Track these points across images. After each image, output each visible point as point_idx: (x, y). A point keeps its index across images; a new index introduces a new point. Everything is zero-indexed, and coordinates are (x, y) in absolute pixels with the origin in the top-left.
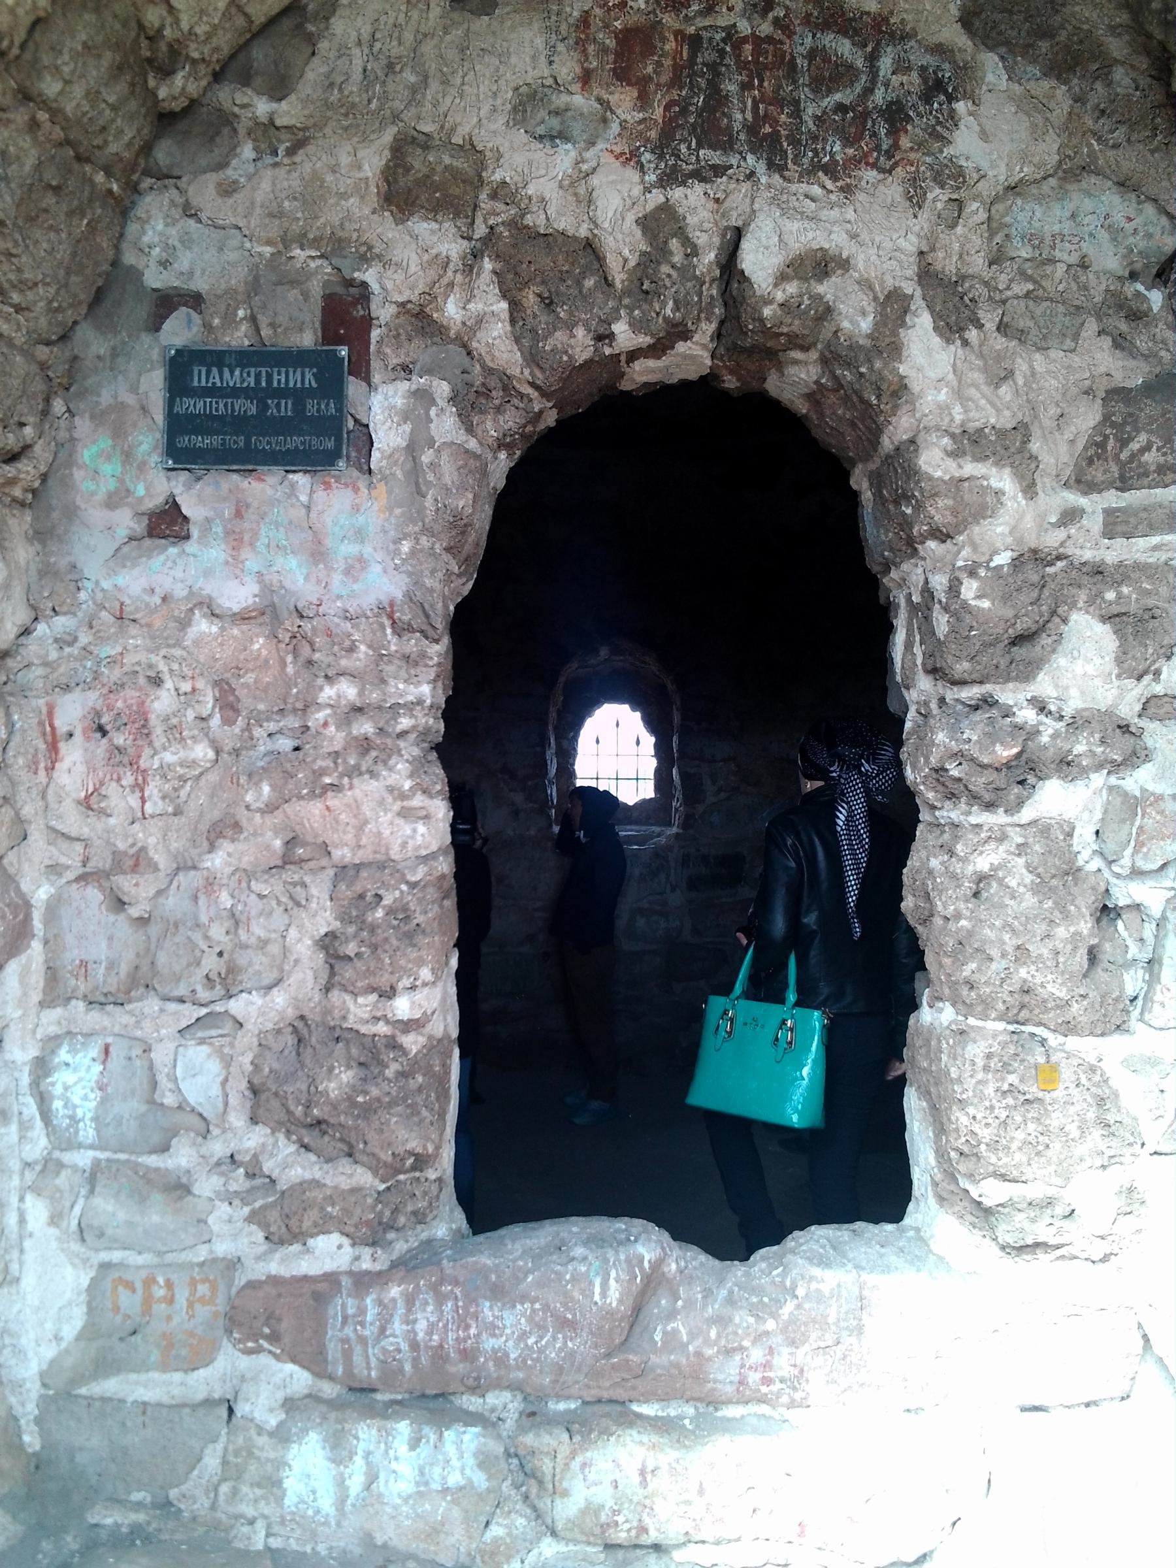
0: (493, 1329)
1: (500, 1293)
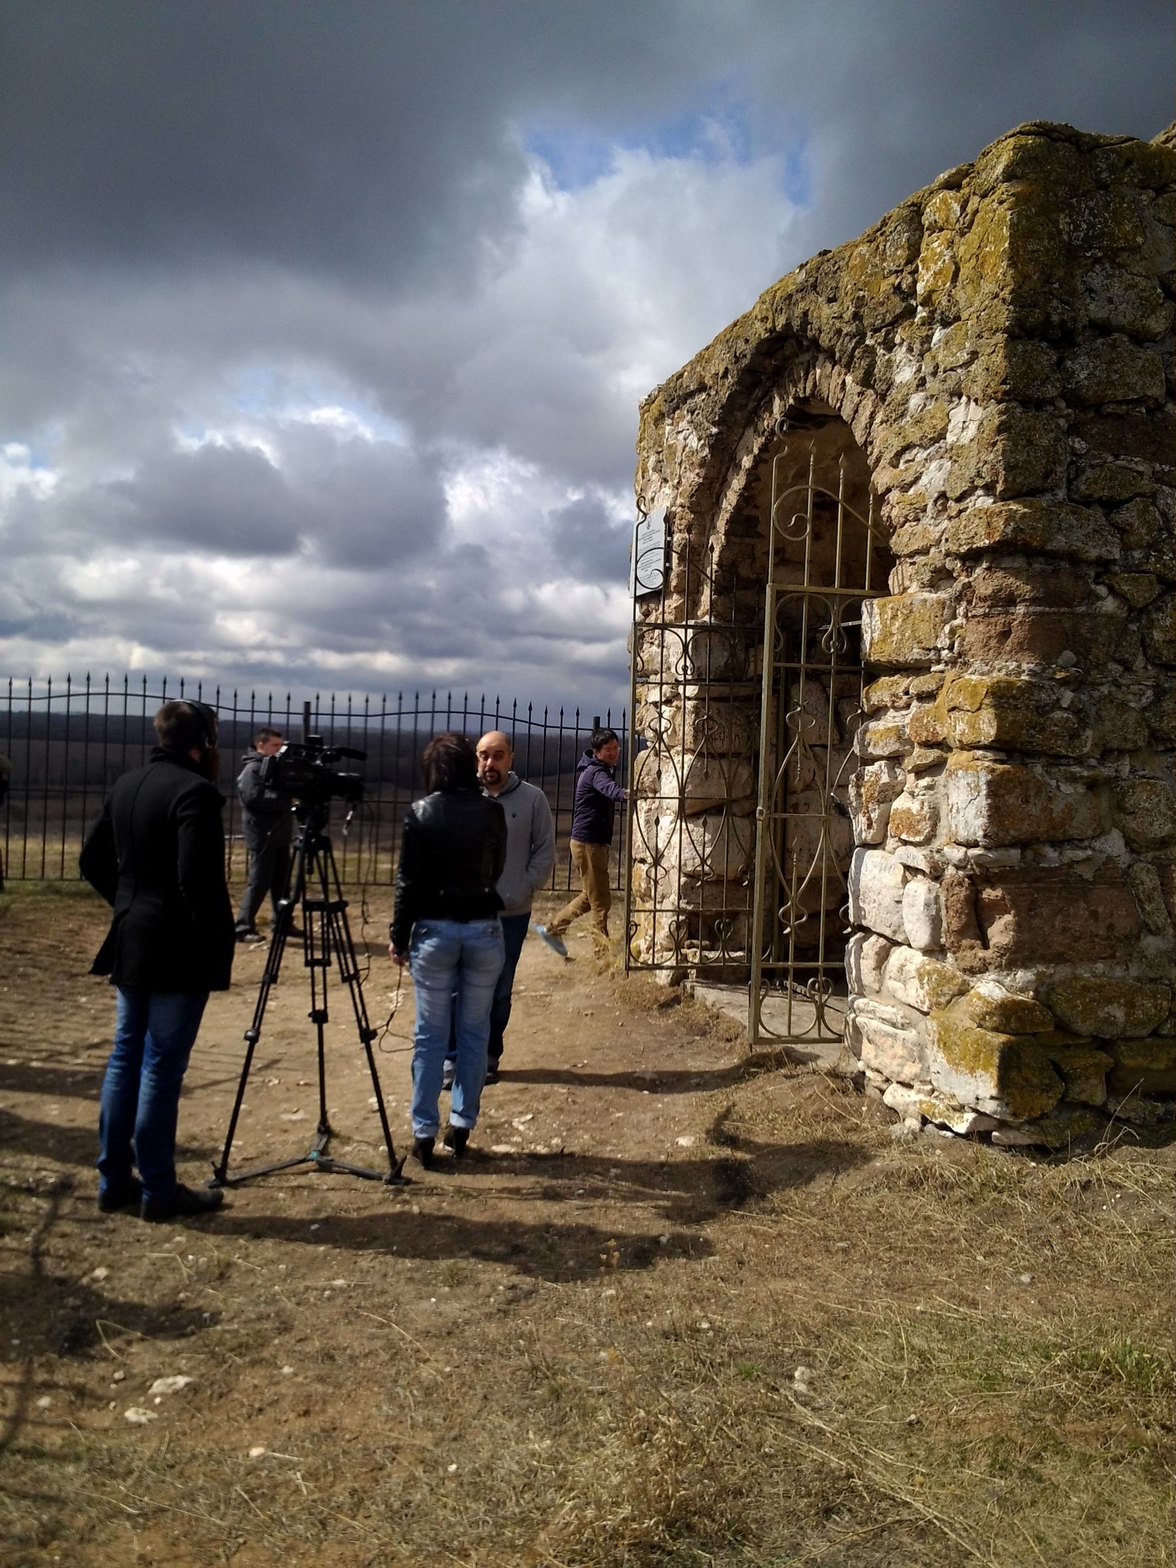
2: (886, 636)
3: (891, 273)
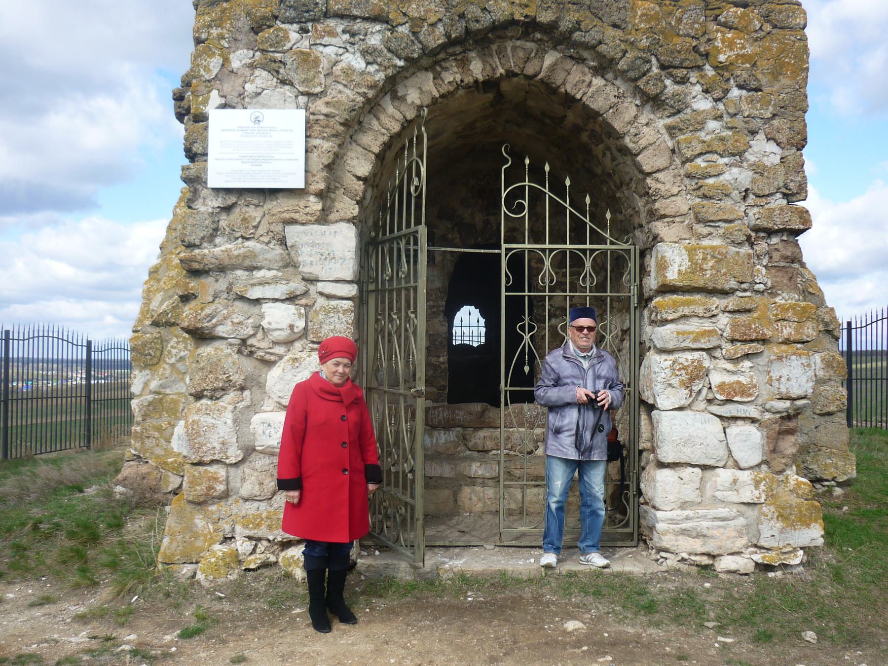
0: (458, 415)
1: (459, 409)
2: (696, 268)
3: (688, 35)
